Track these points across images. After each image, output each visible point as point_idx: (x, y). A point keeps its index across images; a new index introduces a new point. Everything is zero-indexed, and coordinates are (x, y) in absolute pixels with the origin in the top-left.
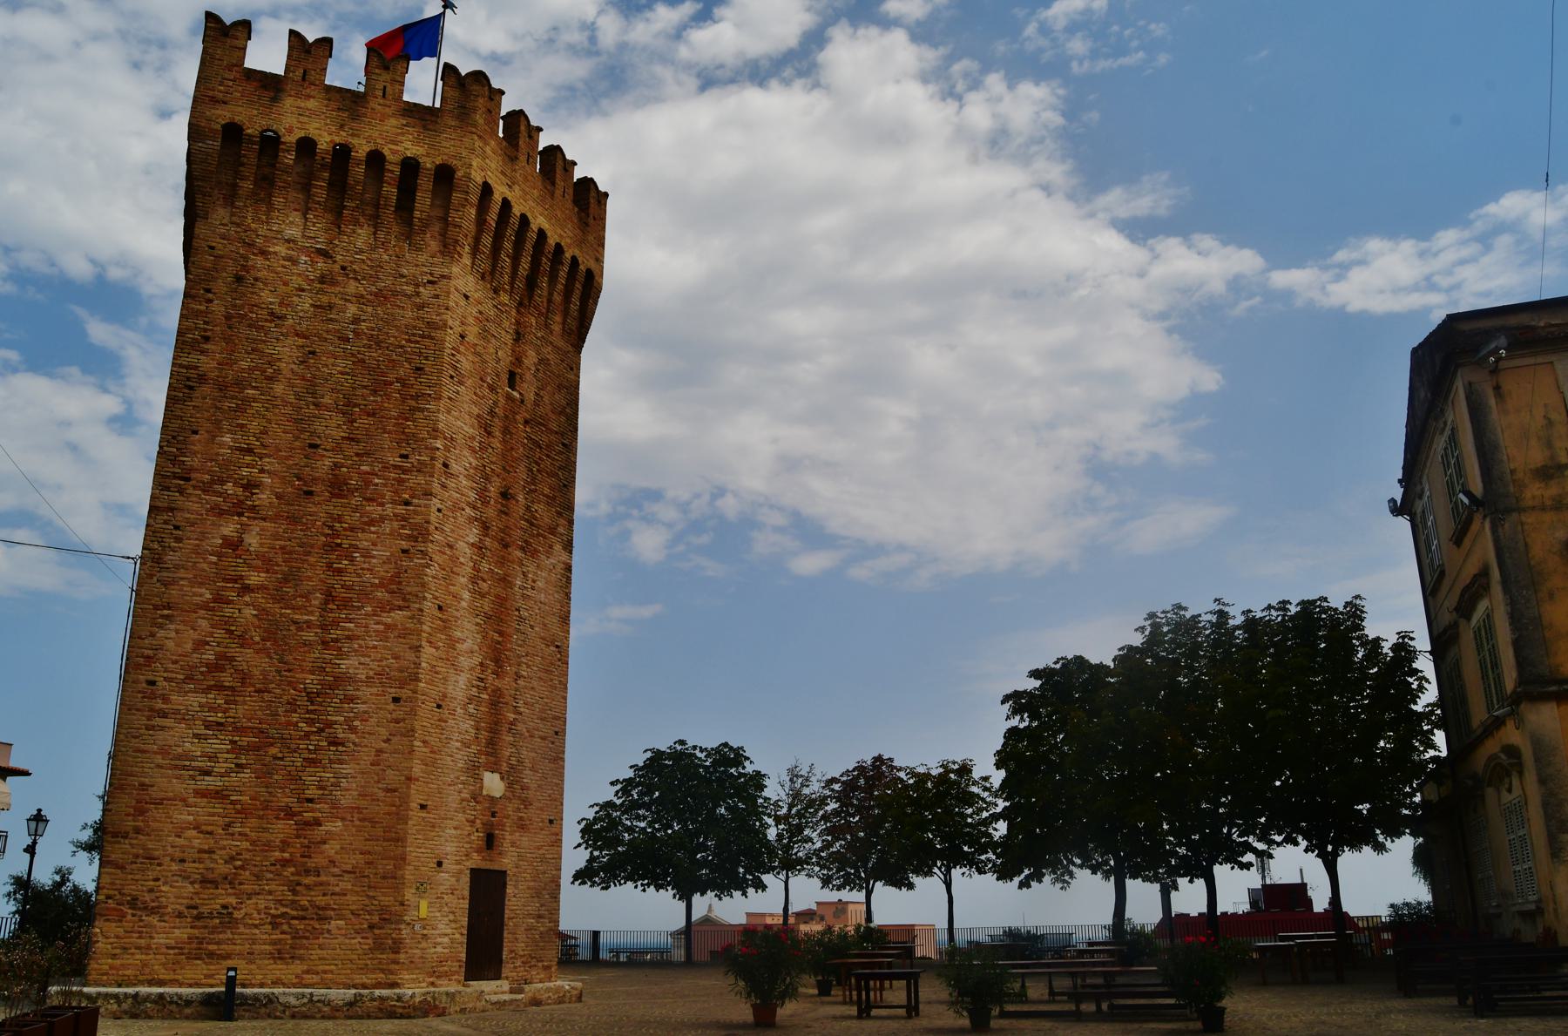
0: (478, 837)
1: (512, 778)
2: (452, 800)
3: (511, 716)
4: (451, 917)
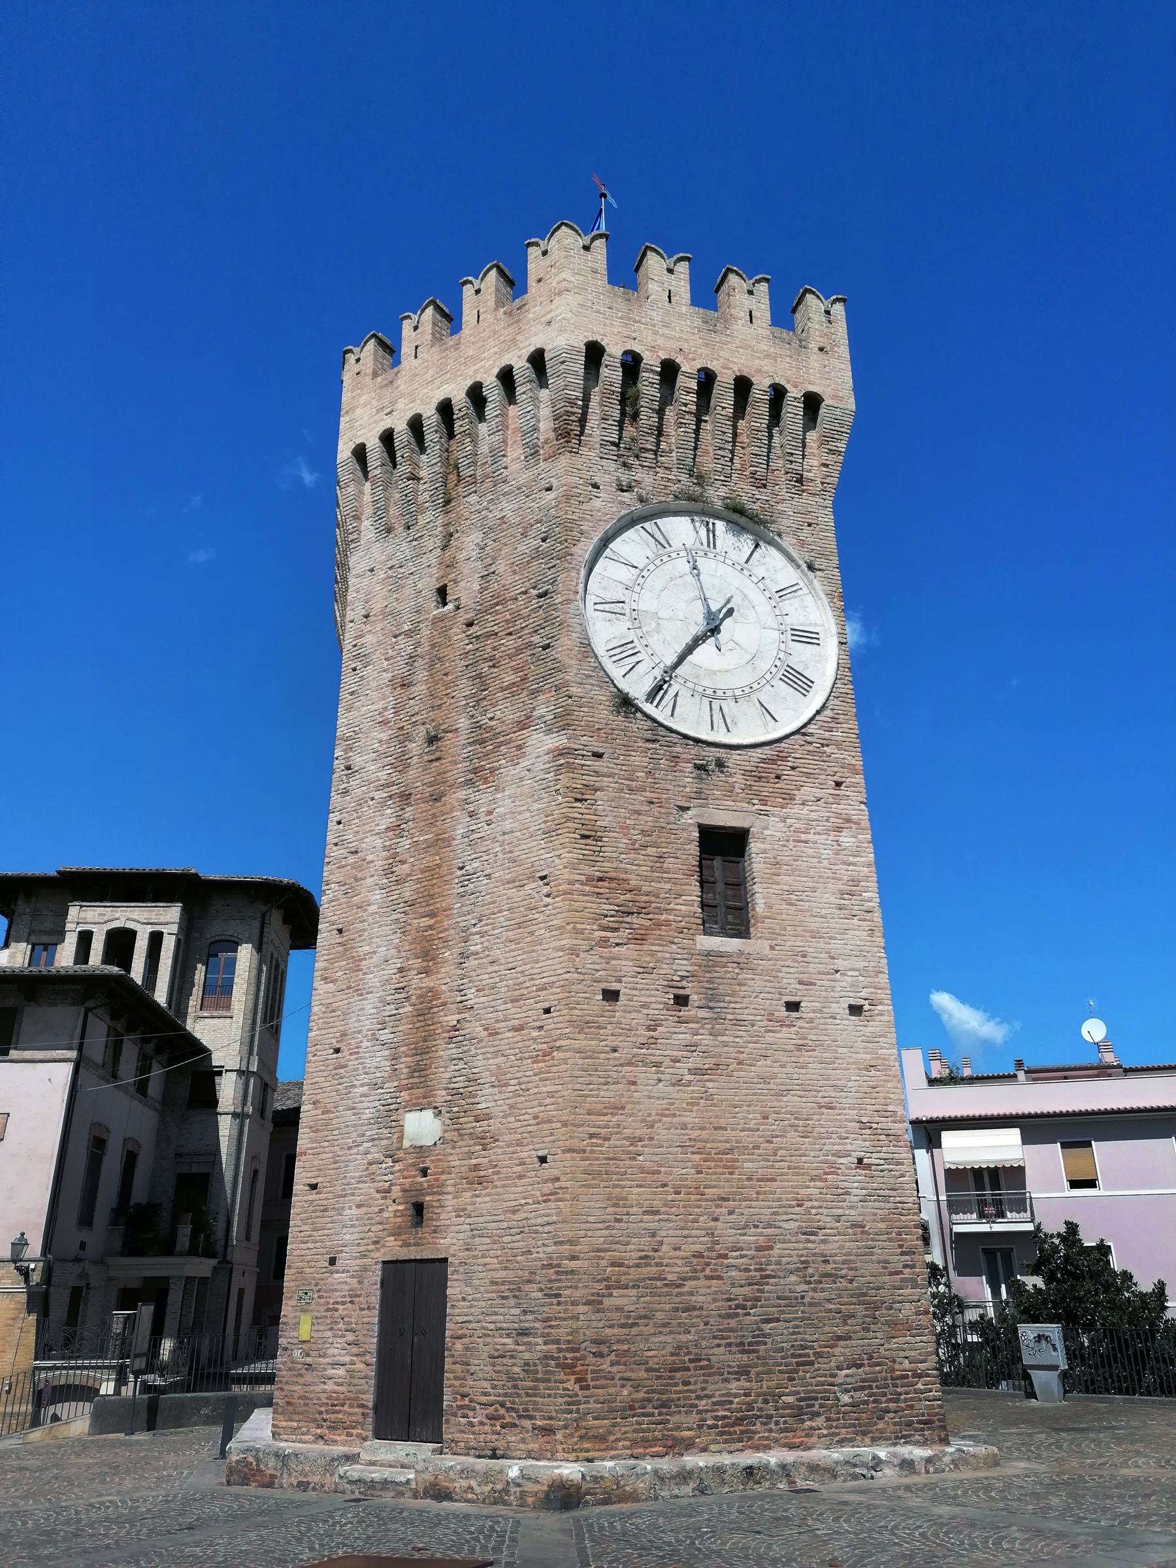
0: (394, 1211)
1: (459, 1110)
3: (452, 1019)
4: (350, 1337)
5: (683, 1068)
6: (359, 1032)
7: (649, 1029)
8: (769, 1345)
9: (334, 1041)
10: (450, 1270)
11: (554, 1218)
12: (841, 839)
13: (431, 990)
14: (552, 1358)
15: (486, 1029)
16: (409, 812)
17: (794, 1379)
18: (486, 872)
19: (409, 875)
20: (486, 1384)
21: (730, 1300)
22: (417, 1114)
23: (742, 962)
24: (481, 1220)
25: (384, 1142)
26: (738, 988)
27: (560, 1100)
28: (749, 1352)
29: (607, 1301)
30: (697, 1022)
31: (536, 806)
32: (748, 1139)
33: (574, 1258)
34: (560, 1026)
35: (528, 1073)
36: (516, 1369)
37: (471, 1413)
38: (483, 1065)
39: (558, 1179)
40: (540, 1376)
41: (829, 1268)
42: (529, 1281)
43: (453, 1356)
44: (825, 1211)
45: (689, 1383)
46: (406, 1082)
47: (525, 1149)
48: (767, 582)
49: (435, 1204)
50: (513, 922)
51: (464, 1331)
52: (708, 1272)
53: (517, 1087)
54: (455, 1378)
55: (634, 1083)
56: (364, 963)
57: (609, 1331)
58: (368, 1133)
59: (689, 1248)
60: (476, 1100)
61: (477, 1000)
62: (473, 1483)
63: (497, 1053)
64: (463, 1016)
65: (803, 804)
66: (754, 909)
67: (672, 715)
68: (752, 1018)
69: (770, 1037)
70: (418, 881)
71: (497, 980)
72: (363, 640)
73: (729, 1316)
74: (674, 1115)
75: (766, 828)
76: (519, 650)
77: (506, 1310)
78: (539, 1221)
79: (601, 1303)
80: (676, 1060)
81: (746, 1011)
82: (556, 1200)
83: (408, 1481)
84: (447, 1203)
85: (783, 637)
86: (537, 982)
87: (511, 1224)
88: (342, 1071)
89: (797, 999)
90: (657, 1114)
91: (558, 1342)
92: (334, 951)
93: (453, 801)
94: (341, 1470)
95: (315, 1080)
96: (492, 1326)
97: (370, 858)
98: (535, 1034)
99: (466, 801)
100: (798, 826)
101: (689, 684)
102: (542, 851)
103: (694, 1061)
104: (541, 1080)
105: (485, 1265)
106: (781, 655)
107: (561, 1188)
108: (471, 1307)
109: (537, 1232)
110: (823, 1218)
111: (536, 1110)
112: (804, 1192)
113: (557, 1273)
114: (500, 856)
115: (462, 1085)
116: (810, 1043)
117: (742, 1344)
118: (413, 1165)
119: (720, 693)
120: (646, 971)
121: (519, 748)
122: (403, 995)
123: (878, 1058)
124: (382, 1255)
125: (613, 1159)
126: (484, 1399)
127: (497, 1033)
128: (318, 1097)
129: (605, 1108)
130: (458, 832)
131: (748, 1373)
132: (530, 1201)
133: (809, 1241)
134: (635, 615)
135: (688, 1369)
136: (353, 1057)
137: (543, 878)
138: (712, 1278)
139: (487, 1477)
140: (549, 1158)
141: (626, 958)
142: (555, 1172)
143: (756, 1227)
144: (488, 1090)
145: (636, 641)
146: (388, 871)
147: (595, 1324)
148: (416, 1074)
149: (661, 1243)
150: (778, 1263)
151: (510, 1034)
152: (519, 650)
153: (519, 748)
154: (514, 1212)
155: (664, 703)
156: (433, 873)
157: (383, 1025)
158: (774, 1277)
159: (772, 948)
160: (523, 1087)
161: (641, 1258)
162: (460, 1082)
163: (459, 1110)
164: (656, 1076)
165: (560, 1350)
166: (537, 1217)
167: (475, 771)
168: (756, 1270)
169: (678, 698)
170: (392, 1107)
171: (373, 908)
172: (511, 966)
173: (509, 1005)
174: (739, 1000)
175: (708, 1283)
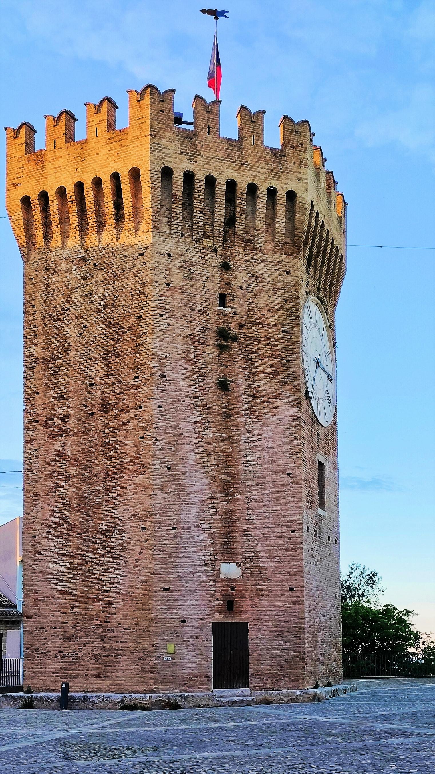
0: (218, 603)
3: (245, 526)
4: (198, 652)
6: (188, 522)
9: (172, 524)
11: (298, 611)
16: (210, 418)
19: (212, 451)
20: (268, 667)
24: (264, 609)
34: (299, 539)
39: (300, 597)
42: (288, 632)
50: (275, 490)
58: (198, 569)
63: (268, 545)
64: (250, 526)
70: (219, 456)
71: (268, 514)
76: (272, 356)
78: (291, 611)
82: (299, 604)
86: (288, 519)
87: (278, 612)
88: (179, 538)
91: (300, 652)
95: (162, 540)
97: (186, 434)
105: (266, 626)
108: (261, 640)
111: (289, 570)
114: (267, 457)
121: (276, 408)
124: (212, 620)
127: (269, 537)
128: (165, 549)
142: (298, 594)
151: (275, 538)
154: (280, 607)
157: (203, 521)
160: (282, 560)
162: (249, 554)
163: (250, 567)
165: (300, 655)
166: (290, 609)
167: (250, 410)
171: (190, 462)
172: (274, 509)
173: (274, 526)
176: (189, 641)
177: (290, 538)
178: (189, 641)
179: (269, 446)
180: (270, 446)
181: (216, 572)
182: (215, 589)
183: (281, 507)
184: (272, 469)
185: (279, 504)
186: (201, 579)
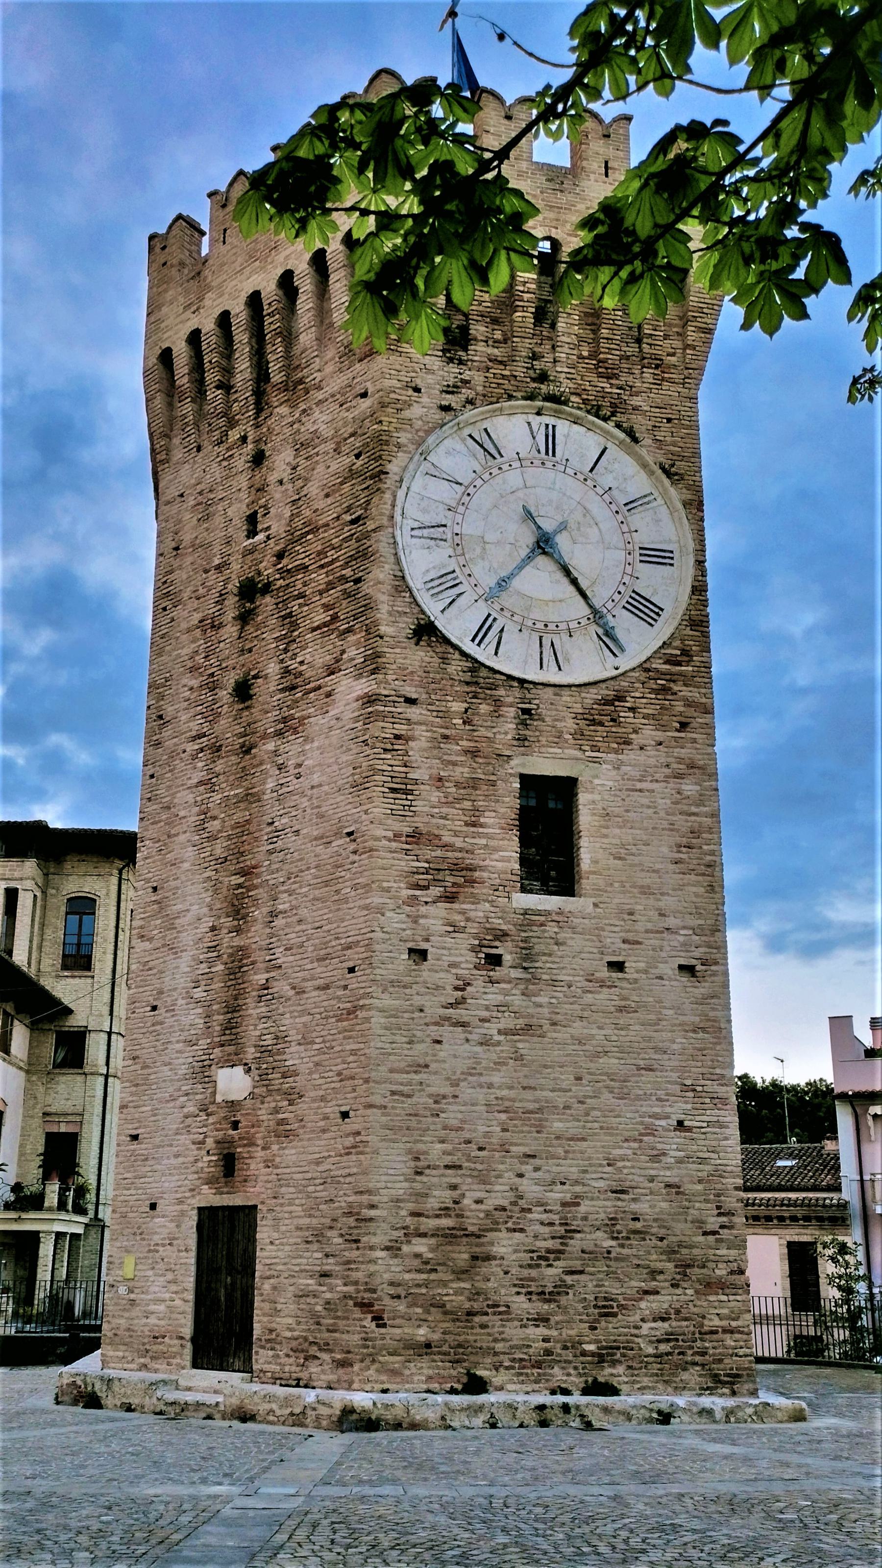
0: (208, 1162)
1: (268, 1068)
2: (172, 1120)
5: (492, 1029)
6: (175, 989)
7: (457, 989)
8: (571, 1296)
10: (259, 1216)
11: (355, 1170)
12: (684, 787)
13: (241, 948)
14: (351, 1298)
15: (294, 988)
17: (595, 1328)
18: (294, 829)
20: (290, 1320)
21: (533, 1251)
22: (229, 1069)
23: (561, 918)
24: (288, 1170)
25: (199, 1097)
26: (556, 947)
27: (362, 1058)
28: (549, 1301)
29: (405, 1248)
30: (509, 982)
31: (345, 758)
32: (560, 1100)
33: (372, 1207)
34: (363, 985)
35: (332, 1032)
36: (319, 1308)
37: (278, 1347)
38: (291, 1023)
39: (358, 1133)
40: (339, 1314)
41: (638, 1225)
42: (331, 1228)
43: (262, 1295)
44: (638, 1171)
45: (486, 1327)
46: (218, 1039)
47: (330, 1104)
48: (614, 492)
49: (245, 1155)
50: (319, 880)
51: (272, 1272)
52: (510, 1225)
53: (322, 1045)
54: (264, 1315)
55: (439, 1042)
56: (177, 921)
57: (407, 1276)
58: (184, 1088)
59: (490, 1203)
60: (284, 1057)
61: (285, 959)
62: (274, 1406)
64: (272, 974)
65: (641, 748)
66: (579, 865)
67: (496, 653)
68: (571, 978)
69: (589, 998)
70: (229, 837)
72: (171, 577)
73: (530, 1266)
74: (481, 1074)
75: (597, 777)
76: (330, 586)
77: (309, 1254)
78: (339, 1173)
79: (399, 1249)
80: (483, 1020)
81: (564, 972)
83: (217, 1404)
84: (256, 1154)
85: (630, 559)
86: (343, 941)
87: (315, 1175)
88: (158, 1027)
89: (621, 959)
90: (463, 1073)
91: (356, 1283)
92: (148, 909)
93: (262, 753)
94: (159, 1394)
95: (135, 1036)
96: (297, 1268)
98: (340, 993)
99: (276, 753)
100: (633, 773)
101: (516, 618)
102: (349, 806)
103: (507, 1022)
104: (344, 1038)
106: (626, 579)
107: (362, 1142)
108: (278, 1250)
109: (339, 1182)
110: (636, 1178)
111: (340, 1067)
112: (617, 1152)
113: (357, 1220)
114: (309, 811)
115: (270, 1042)
116: (633, 1004)
117: (543, 1293)
118: (225, 1118)
119: (552, 627)
120: (456, 929)
121: (329, 695)
122: (215, 954)
123: (709, 1020)
125: (416, 1115)
126: (288, 1334)
127: (304, 992)
128: (138, 1053)
129: (409, 1066)
130: (268, 786)
131: (547, 1320)
132: (333, 1154)
133: (619, 1199)
134: (457, 540)
135: (487, 1314)
136: (168, 1015)
137: (350, 834)
138: (515, 1230)
139: (287, 1401)
140: (352, 1114)
141: (436, 916)
142: (356, 1127)
143: (563, 1184)
144: (294, 1048)
145: (457, 570)
146: (201, 827)
147: (393, 1269)
148: (228, 1032)
149: (463, 1196)
150: (585, 1219)
151: (316, 993)
152: (330, 586)
153: (329, 695)
154: (318, 1164)
155: (486, 640)
156: (243, 829)
157: (196, 984)
158: (579, 1232)
159: (595, 905)
161: (440, 1209)
162: (269, 1040)
163: (268, 1068)
164: (463, 1036)
165: (358, 1291)
166: (338, 1169)
167: (285, 720)
168: (561, 1224)
169: (504, 635)
170: (206, 1063)
171: (186, 866)
172: (317, 925)
173: (316, 964)
174: (557, 960)
175: (510, 1235)
176: (157, 1251)
177: (345, 987)
178: (157, 1251)
179: (313, 783)
180: (315, 782)
181: (210, 1090)
182: (205, 1129)
183: (330, 915)
184: (315, 833)
185: (326, 911)
186: (185, 1110)
